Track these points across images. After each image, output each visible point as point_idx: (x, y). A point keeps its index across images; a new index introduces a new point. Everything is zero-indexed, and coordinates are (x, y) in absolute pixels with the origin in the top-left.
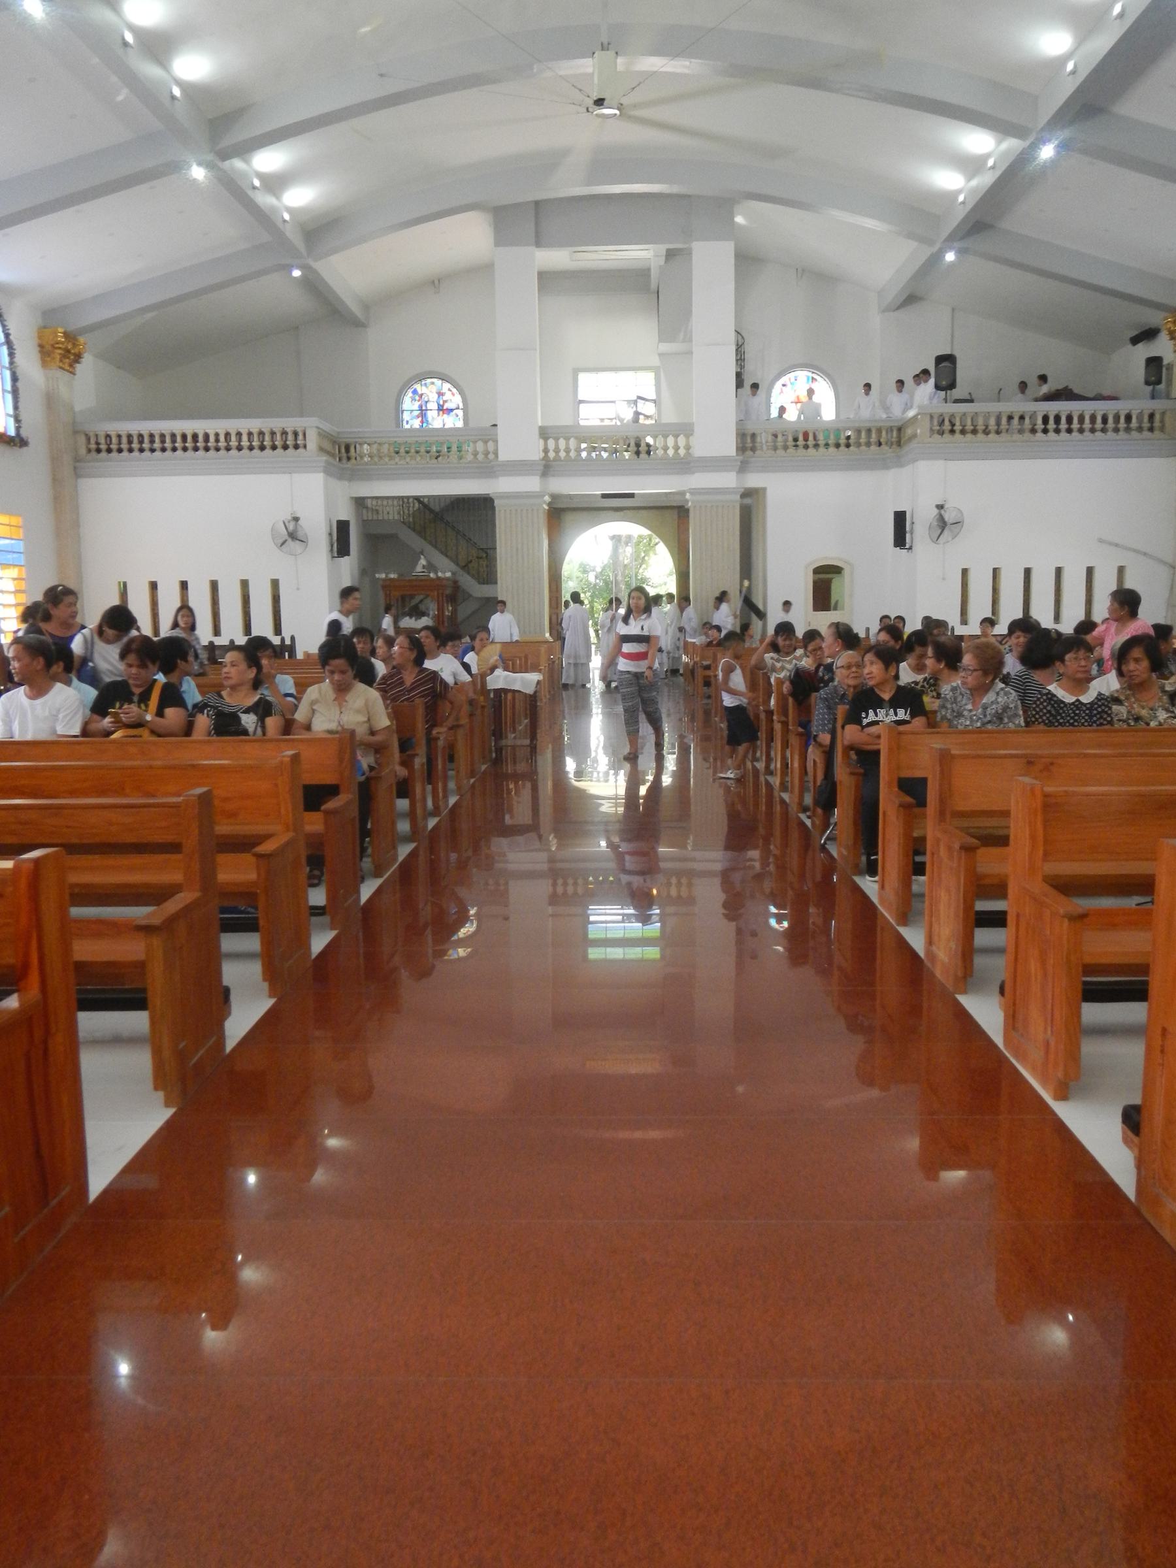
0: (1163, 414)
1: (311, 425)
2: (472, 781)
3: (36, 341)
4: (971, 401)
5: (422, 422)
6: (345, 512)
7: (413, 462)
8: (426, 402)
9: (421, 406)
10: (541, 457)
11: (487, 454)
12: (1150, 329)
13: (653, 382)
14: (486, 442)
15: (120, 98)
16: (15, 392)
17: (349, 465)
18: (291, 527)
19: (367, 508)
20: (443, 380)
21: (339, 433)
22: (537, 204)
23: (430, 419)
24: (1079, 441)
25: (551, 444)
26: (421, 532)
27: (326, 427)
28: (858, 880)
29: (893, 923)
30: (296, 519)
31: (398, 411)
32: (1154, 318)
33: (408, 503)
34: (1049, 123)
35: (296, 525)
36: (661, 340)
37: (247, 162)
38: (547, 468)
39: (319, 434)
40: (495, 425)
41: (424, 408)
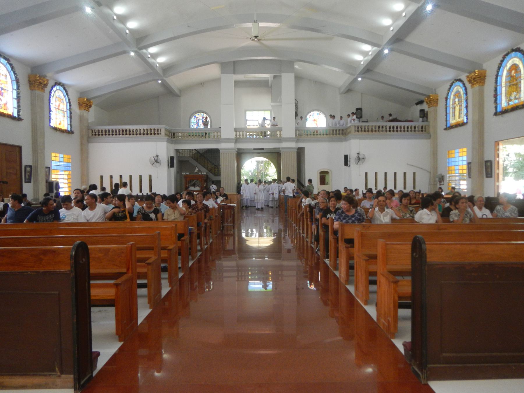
0: (425, 126)
1: (163, 127)
2: (216, 235)
3: (78, 101)
4: (367, 122)
5: (197, 126)
6: (173, 154)
7: (194, 138)
9: (197, 121)
10: (235, 137)
11: (218, 136)
13: (270, 114)
14: (217, 133)
15: (110, 32)
16: (71, 117)
17: (174, 139)
18: (156, 158)
19: (179, 152)
20: (204, 113)
21: (171, 130)
22: (234, 62)
23: (200, 125)
25: (238, 133)
27: (168, 128)
28: (325, 260)
29: (333, 270)
30: (157, 156)
31: (190, 122)
32: (422, 98)
33: (192, 151)
34: (386, 44)
35: (157, 158)
36: (272, 102)
37: (155, 60)
38: (237, 140)
39: (165, 130)
40: (220, 127)
41: (198, 121)
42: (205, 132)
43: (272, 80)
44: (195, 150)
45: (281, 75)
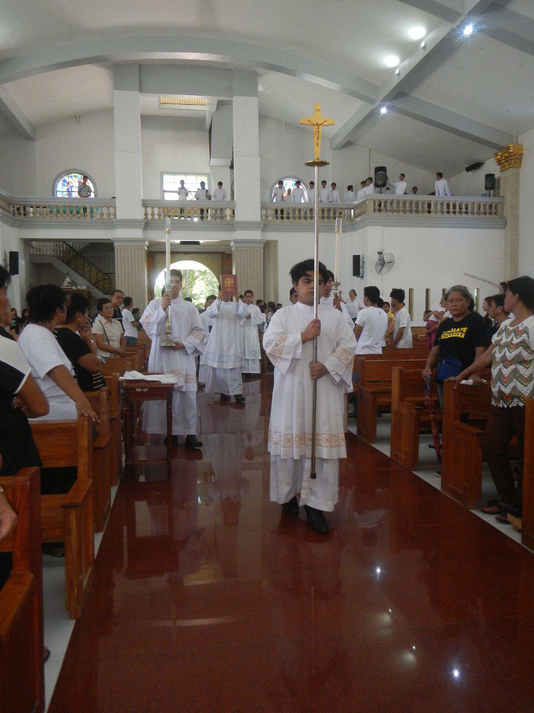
0: (496, 205)
8: (72, 187)
9: (68, 189)
10: (143, 218)
11: (109, 215)
12: (478, 162)
14: (108, 208)
19: (33, 247)
21: (13, 198)
24: (454, 218)
25: (149, 210)
26: (68, 263)
31: (54, 191)
38: (147, 225)
40: (114, 198)
41: (70, 190)
42: (83, 205)
43: (213, 113)
44: (65, 241)
45: (232, 101)
